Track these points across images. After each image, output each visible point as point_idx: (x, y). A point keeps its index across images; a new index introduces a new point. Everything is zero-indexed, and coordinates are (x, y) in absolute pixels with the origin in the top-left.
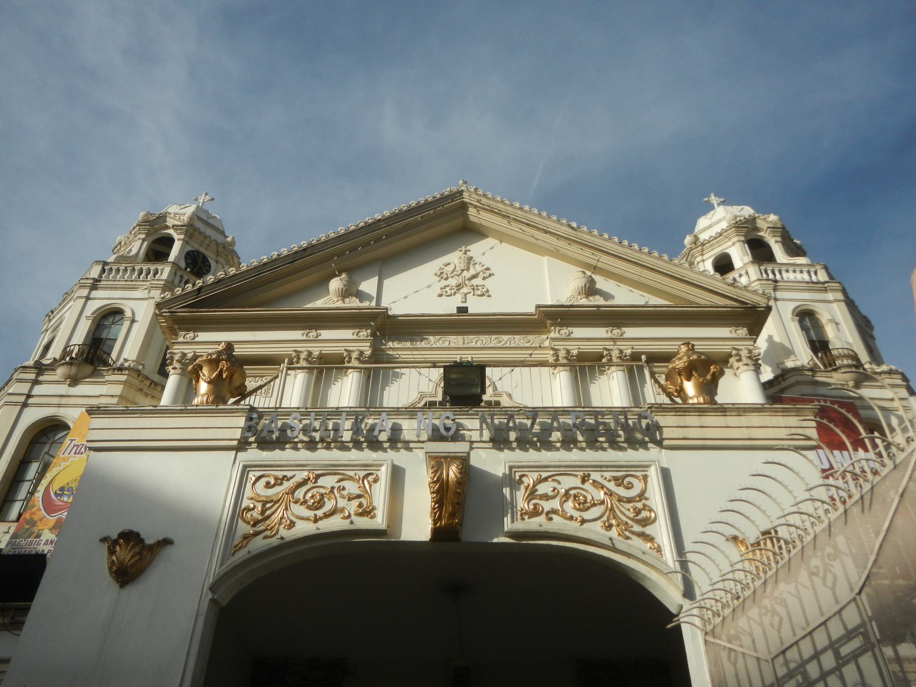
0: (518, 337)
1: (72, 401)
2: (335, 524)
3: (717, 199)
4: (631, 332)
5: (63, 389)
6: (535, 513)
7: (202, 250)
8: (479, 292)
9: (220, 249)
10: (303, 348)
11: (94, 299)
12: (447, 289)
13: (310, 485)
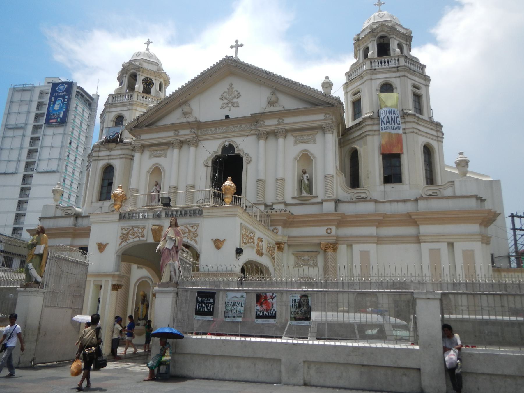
0: (247, 125)
1: (112, 157)
2: (137, 239)
4: (287, 120)
7: (149, 76)
8: (235, 105)
9: (156, 74)
11: (112, 112)
12: (224, 105)
13: (132, 230)
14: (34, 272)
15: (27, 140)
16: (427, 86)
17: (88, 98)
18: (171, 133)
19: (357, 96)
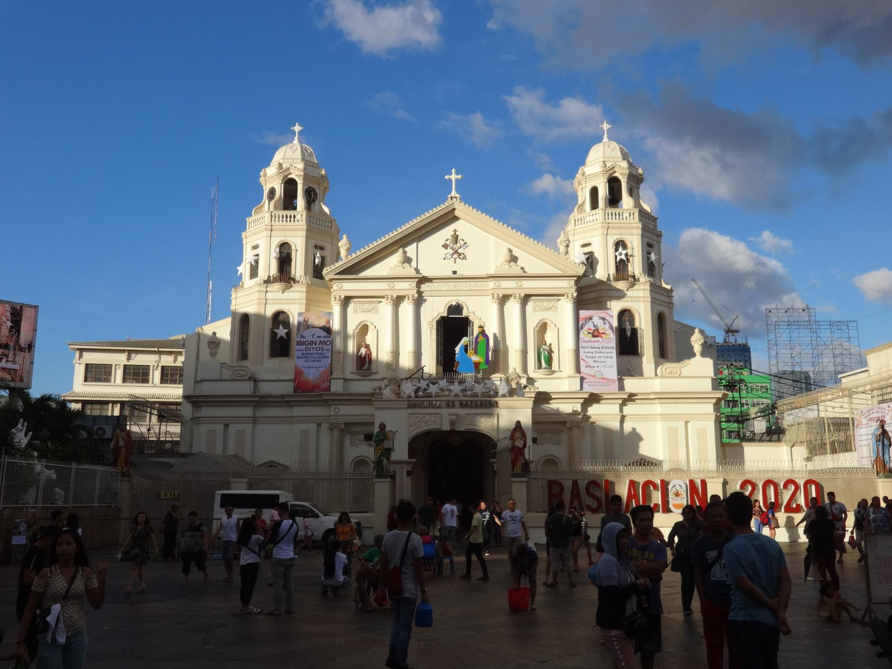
2: (430, 427)
3: (607, 125)
5: (279, 295)
6: (471, 424)
8: (461, 257)
10: (389, 293)
12: (448, 255)
16: (659, 242)
19: (587, 249)
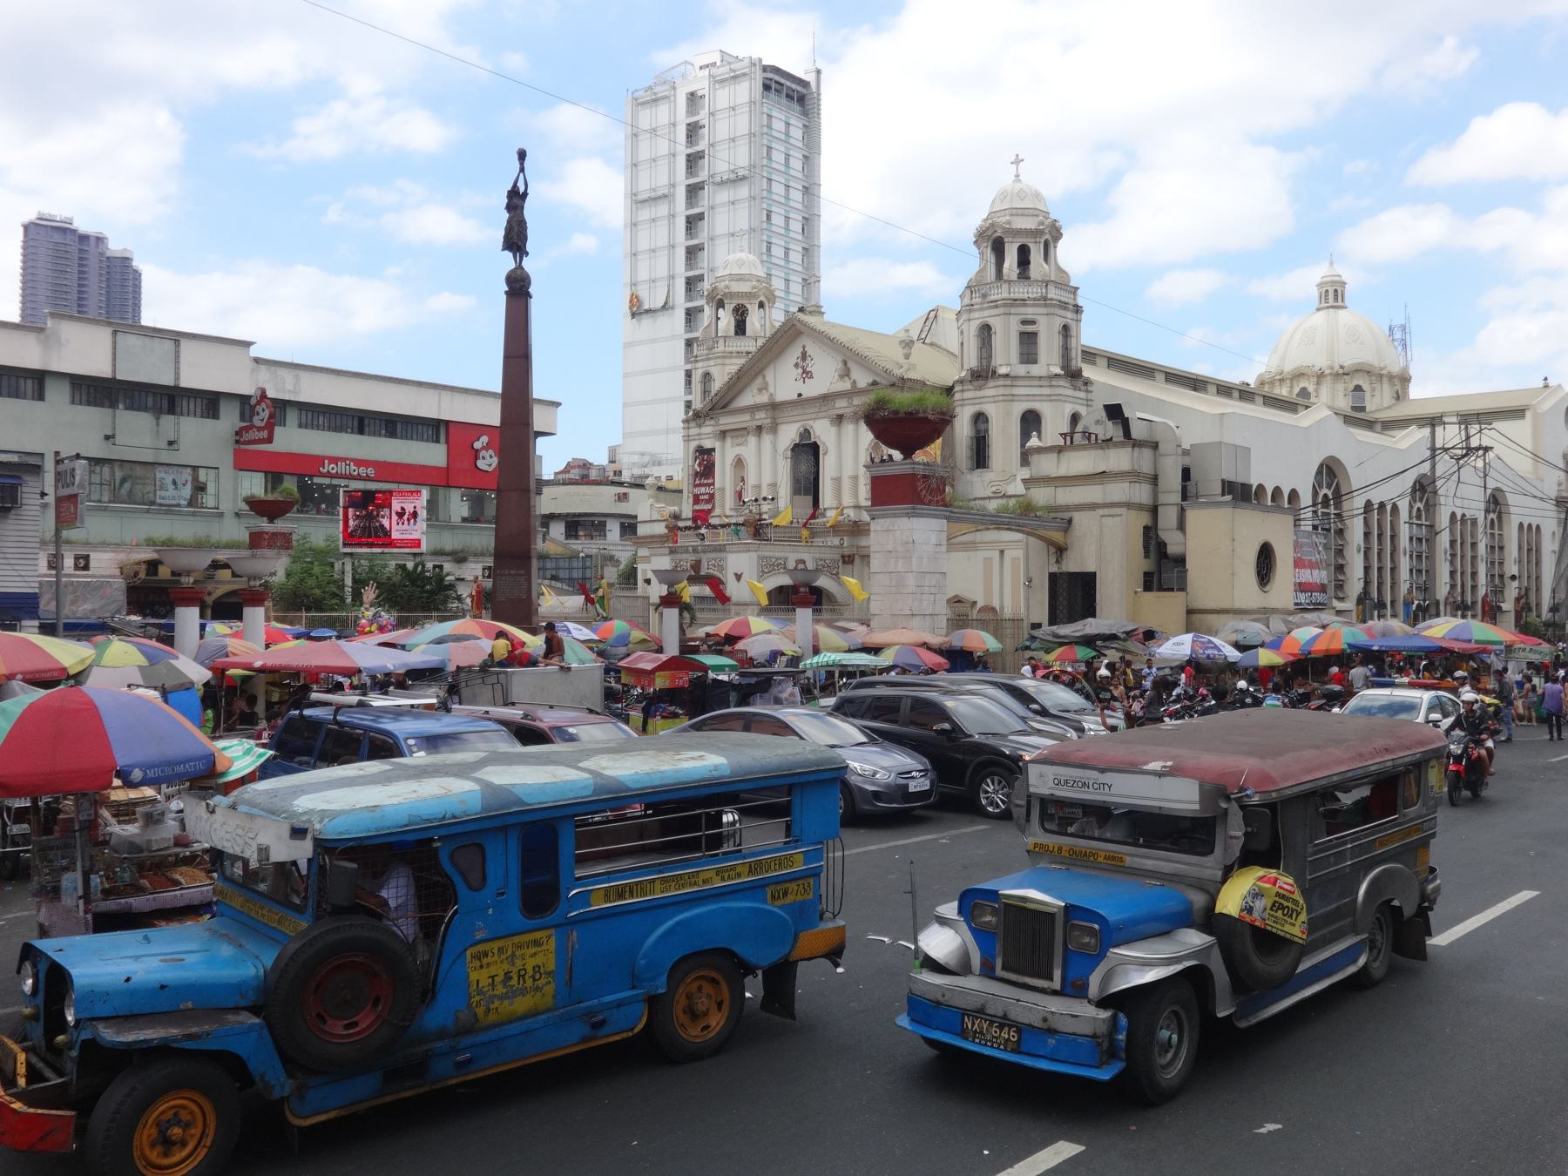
7: (740, 302)
10: (749, 424)
14: (601, 611)
15: (681, 224)
17: (794, 86)
18: (746, 417)
